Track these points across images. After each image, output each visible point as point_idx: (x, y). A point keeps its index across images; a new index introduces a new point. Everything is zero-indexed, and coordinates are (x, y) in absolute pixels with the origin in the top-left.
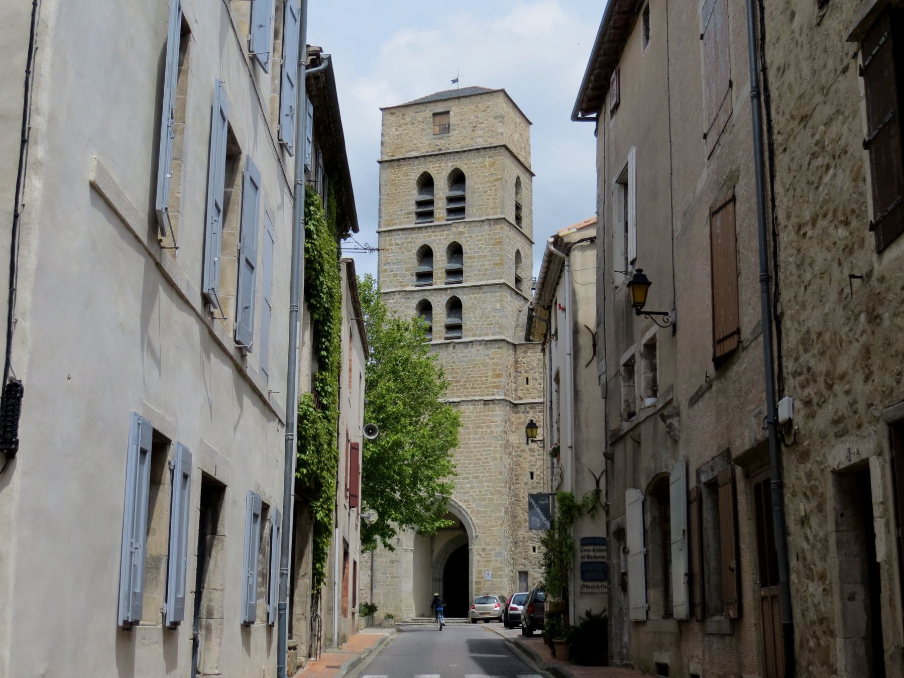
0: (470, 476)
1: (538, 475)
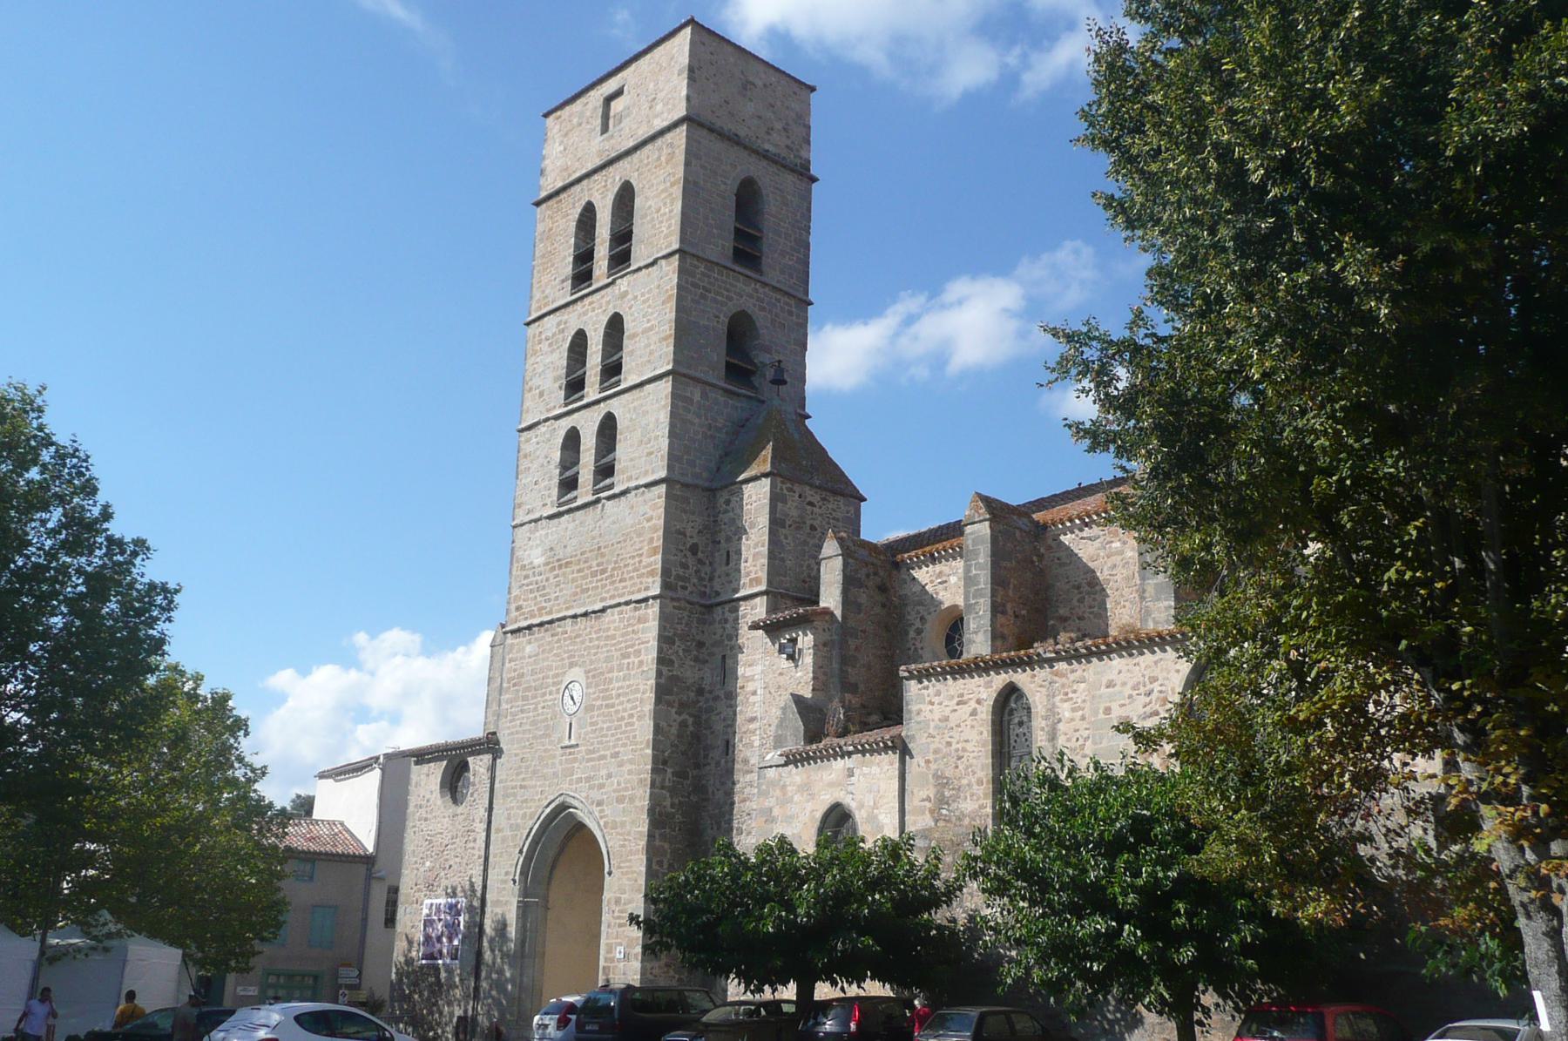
0: (608, 753)
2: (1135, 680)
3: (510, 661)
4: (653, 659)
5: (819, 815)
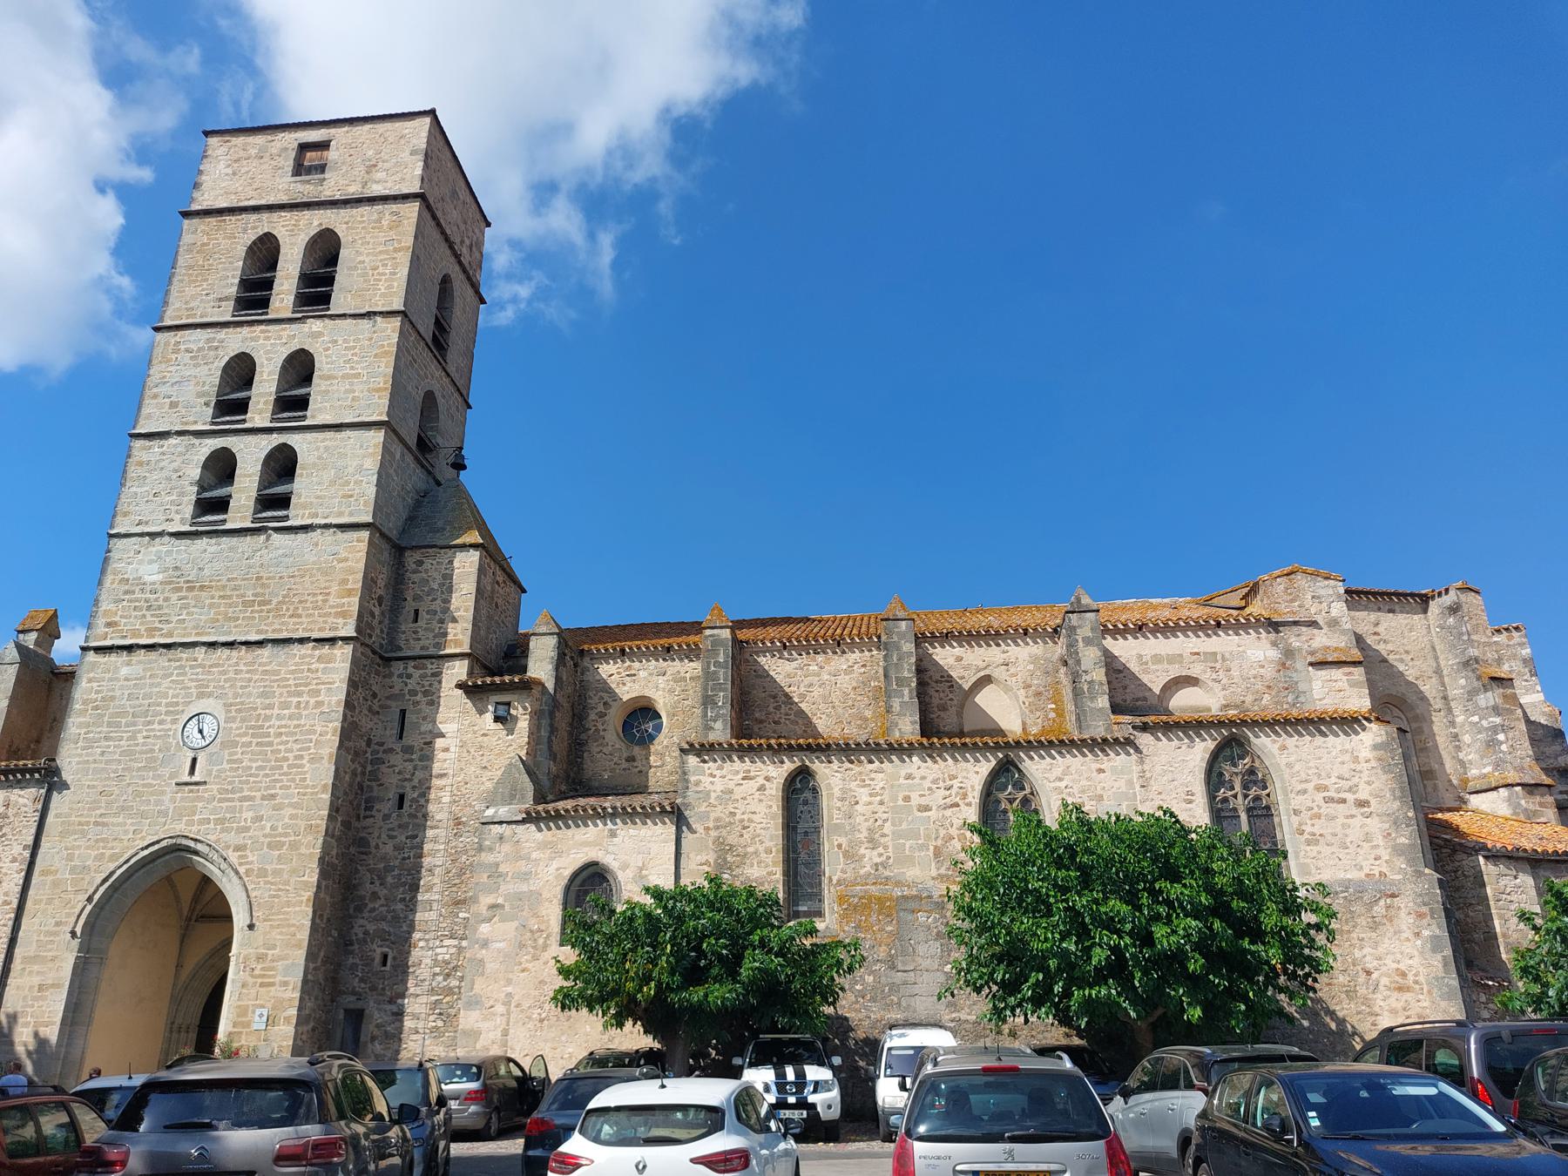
0: (258, 794)
1: (413, 800)
2: (935, 776)
3: (90, 681)
4: (338, 702)
5: (568, 873)
